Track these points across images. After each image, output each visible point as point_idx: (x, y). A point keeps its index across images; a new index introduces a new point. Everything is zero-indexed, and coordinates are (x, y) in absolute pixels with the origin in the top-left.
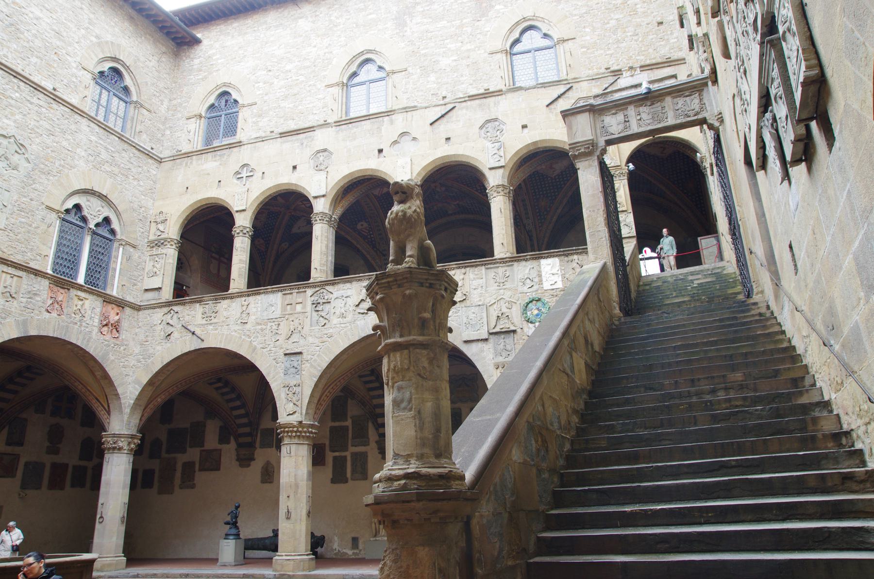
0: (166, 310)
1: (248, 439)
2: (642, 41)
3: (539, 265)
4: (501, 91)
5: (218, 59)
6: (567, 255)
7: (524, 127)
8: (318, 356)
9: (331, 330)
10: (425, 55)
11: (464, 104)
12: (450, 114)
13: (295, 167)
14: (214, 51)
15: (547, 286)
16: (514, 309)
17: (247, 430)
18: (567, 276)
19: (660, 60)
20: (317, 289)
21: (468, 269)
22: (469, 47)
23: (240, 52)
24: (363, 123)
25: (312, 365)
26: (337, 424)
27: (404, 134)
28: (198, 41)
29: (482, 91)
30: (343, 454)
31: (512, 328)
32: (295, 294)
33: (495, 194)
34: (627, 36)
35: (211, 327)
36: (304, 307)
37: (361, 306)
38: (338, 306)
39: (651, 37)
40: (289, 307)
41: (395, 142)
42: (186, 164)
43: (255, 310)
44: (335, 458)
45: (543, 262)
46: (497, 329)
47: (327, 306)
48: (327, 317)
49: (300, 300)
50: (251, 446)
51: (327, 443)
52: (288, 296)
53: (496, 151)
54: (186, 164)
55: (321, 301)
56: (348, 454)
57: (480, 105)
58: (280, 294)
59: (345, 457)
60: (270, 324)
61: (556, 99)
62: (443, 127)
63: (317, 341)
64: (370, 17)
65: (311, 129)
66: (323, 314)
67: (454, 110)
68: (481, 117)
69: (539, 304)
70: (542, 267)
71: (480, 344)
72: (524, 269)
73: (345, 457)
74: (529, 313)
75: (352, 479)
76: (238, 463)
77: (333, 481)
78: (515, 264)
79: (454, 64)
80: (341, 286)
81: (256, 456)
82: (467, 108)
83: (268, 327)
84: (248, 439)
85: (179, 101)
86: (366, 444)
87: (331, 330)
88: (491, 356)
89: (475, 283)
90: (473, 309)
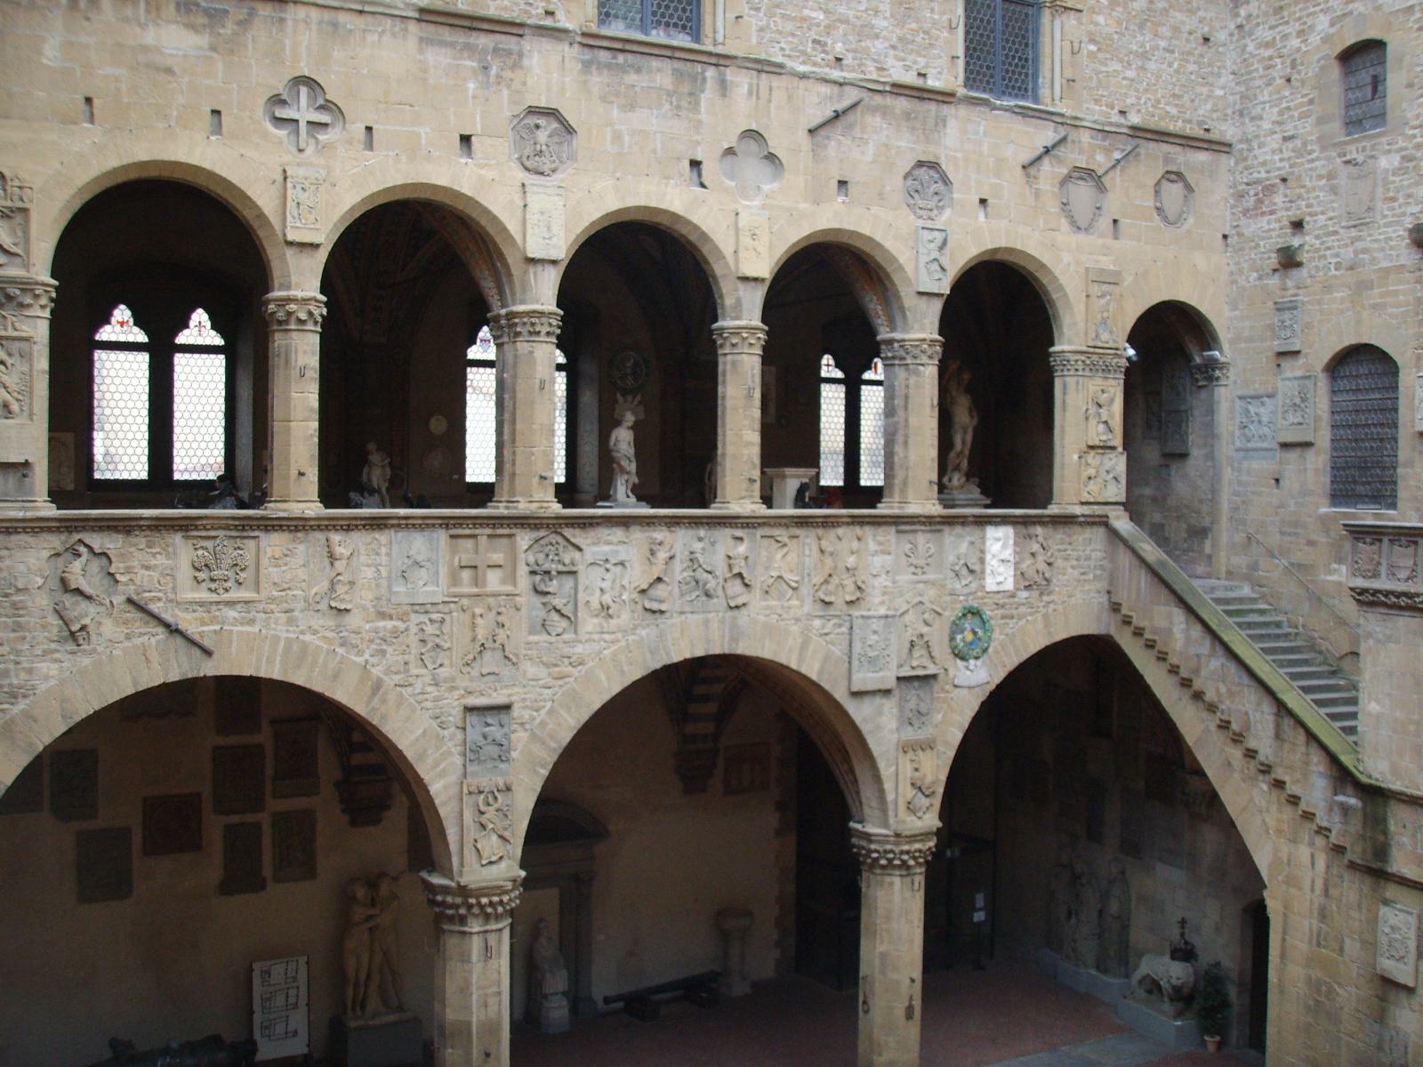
0: (56, 541)
2: (1177, 71)
3: (983, 538)
4: (952, 95)
7: (983, 202)
8: (551, 712)
9: (579, 649)
11: (878, 99)
12: (851, 117)
13: (466, 140)
15: (990, 584)
16: (937, 624)
18: (1024, 566)
20: (542, 533)
24: (655, 63)
25: (534, 737)
26: (232, 740)
27: (751, 134)
30: (250, 818)
31: (932, 670)
32: (483, 540)
33: (924, 359)
34: (1156, 48)
35: (232, 614)
36: (512, 578)
37: (652, 592)
38: (594, 584)
39: (1191, 67)
40: (466, 575)
41: (730, 152)
44: (230, 830)
47: (569, 583)
48: (567, 610)
49: (497, 557)
53: (935, 254)
55: (554, 567)
56: (264, 819)
59: (258, 826)
60: (415, 618)
61: (1039, 158)
63: (542, 672)
66: (558, 602)
67: (859, 109)
68: (908, 147)
69: (977, 620)
70: (988, 543)
71: (878, 700)
72: (957, 543)
74: (959, 637)
75: (277, 880)
77: (229, 886)
78: (947, 529)
83: (414, 629)
87: (579, 649)
88: (894, 725)
89: (878, 561)
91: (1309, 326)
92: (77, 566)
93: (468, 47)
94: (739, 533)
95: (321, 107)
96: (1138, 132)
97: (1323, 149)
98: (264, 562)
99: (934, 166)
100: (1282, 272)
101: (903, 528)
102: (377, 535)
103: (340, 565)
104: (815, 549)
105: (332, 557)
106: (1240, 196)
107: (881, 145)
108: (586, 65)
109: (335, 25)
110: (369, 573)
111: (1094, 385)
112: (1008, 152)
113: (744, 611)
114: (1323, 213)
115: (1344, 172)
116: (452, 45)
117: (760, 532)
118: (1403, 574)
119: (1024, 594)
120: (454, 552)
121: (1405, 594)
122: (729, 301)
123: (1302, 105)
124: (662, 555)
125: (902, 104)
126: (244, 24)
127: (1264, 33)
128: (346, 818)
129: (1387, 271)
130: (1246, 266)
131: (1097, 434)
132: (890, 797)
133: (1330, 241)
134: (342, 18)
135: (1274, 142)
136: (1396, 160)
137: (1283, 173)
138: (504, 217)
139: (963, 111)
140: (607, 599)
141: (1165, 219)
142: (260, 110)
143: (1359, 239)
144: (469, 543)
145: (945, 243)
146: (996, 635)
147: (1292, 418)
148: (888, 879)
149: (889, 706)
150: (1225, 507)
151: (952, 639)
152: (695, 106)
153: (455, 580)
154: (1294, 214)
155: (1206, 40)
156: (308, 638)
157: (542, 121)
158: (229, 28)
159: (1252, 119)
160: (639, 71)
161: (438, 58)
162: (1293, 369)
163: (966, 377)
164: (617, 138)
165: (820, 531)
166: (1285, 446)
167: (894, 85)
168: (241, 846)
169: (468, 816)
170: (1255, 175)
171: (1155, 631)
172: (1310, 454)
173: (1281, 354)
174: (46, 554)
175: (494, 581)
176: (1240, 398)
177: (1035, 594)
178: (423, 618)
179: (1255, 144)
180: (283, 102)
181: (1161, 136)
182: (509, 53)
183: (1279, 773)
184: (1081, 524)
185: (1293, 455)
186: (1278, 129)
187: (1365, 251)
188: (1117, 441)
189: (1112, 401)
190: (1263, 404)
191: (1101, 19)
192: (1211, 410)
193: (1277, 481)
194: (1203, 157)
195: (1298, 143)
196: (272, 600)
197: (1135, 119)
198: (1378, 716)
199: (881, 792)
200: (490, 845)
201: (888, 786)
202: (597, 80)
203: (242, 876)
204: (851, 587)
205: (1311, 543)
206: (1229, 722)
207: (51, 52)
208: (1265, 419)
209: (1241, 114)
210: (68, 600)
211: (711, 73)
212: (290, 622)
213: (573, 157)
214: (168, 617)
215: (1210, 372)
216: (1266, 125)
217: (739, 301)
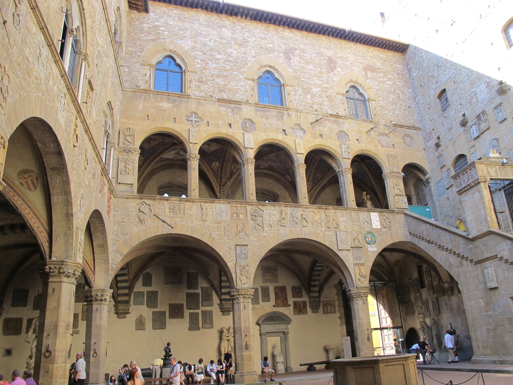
0: (139, 201)
1: (126, 298)
3: (370, 215)
5: (163, 31)
6: (381, 212)
10: (303, 81)
11: (327, 118)
13: (230, 125)
14: (160, 24)
15: (374, 226)
17: (126, 291)
19: (411, 126)
20: (253, 206)
21: (337, 211)
22: (325, 85)
23: (181, 33)
24: (272, 110)
28: (146, 11)
29: (335, 113)
30: (196, 311)
31: (361, 246)
32: (239, 208)
33: (347, 173)
40: (235, 215)
41: (292, 128)
42: (145, 98)
43: (211, 213)
45: (372, 214)
46: (353, 246)
48: (261, 225)
49: (243, 212)
50: (127, 302)
51: (185, 303)
52: (234, 208)
54: (145, 98)
57: (335, 121)
58: (229, 205)
59: (198, 313)
62: (318, 128)
64: (269, 45)
65: (239, 103)
68: (336, 128)
72: (363, 215)
73: (198, 313)
76: (116, 315)
77: (190, 329)
79: (320, 93)
80: (268, 207)
81: (130, 311)
82: (329, 120)
83: (222, 226)
84: (126, 298)
85: (134, 49)
86: (211, 305)
87: (264, 234)
88: (352, 260)
89: (341, 219)
90: (343, 233)
91: (446, 158)
92: (143, 207)
93: (229, 107)
94: (304, 209)
95: (197, 118)
96: (394, 125)
97: (439, 118)
98: (186, 209)
99: (344, 132)
101: (347, 211)
102: (213, 204)
103: (204, 210)
104: (324, 215)
105: (202, 208)
106: (425, 138)
107: (328, 127)
108: (256, 111)
109: (200, 102)
110: (211, 213)
111: (395, 181)
112: (362, 129)
113: (307, 228)
116: (226, 106)
117: (309, 210)
118: (466, 181)
119: (384, 230)
120: (232, 210)
121: (468, 185)
122: (295, 159)
124: (284, 213)
125: (333, 119)
126: (180, 102)
127: (422, 101)
128: (221, 313)
129: (458, 136)
131: (397, 192)
132: (354, 278)
134: (201, 101)
136: (454, 111)
138: (240, 140)
139: (349, 120)
140: (271, 223)
141: (407, 145)
142: (184, 118)
144: (236, 208)
145: (348, 147)
146: (378, 239)
147: (447, 181)
148: (357, 302)
149: (350, 254)
150: (438, 211)
151: (365, 239)
152: (283, 119)
153: (232, 216)
155: (410, 107)
156: (196, 226)
157: (247, 121)
158: (177, 103)
160: (268, 112)
161: (223, 109)
162: (444, 170)
163: (369, 196)
164: (265, 125)
165: (325, 210)
166: (447, 189)
167: (330, 115)
168: (194, 318)
169: (238, 271)
172: (453, 187)
173: (442, 168)
174: (136, 204)
175: (241, 216)
177: (387, 230)
178: (225, 224)
180: (189, 117)
181: (401, 126)
182: (239, 108)
184: (398, 213)
185: (450, 190)
188: (404, 194)
189: (400, 184)
191: (381, 103)
192: (430, 191)
194: (414, 131)
195: (434, 120)
196: (187, 217)
197: (393, 123)
199: (351, 277)
200: (244, 279)
201: (353, 275)
202: (259, 113)
203: (194, 326)
204: (335, 224)
205: (459, 209)
207: (140, 107)
210: (141, 214)
211: (286, 112)
212: (192, 222)
213: (255, 128)
214: (163, 219)
215: (427, 182)
217: (298, 159)
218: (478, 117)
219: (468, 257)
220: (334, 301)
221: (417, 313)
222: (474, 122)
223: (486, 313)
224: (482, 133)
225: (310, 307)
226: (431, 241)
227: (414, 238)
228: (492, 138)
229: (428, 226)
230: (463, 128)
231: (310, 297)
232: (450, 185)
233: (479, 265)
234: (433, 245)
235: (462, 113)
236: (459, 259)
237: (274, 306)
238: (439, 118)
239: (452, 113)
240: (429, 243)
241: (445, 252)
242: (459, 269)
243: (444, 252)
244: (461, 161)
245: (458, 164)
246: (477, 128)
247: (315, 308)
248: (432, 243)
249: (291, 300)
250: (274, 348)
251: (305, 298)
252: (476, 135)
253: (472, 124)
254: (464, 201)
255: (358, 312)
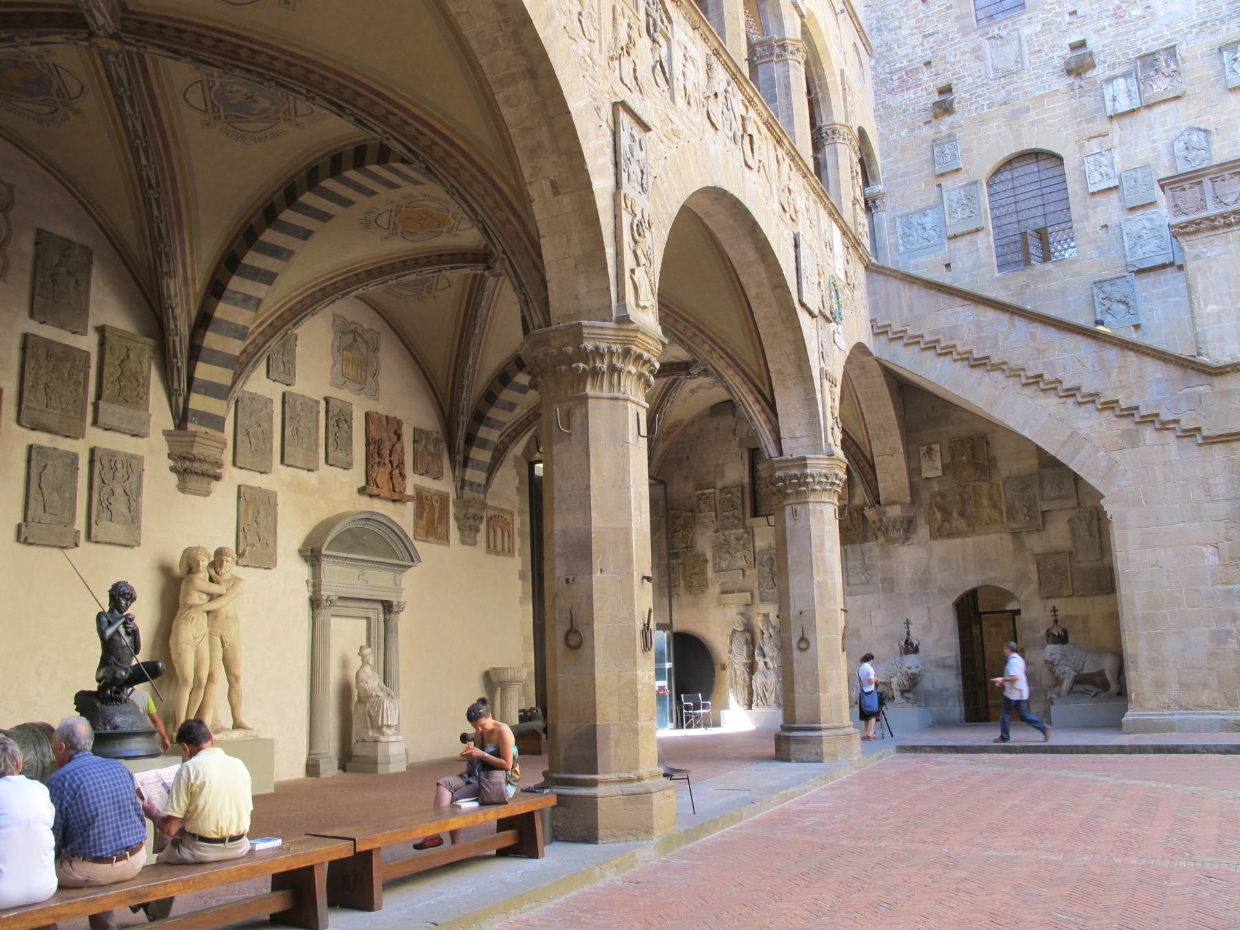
56: (80, 448)
59: (74, 458)
73: (74, 458)
97: (965, 34)
100: (935, 122)
114: (970, 75)
115: (987, 44)
118: (1230, 200)
121: (1234, 212)
123: (939, 12)
128: (174, 478)
130: (896, 126)
133: (979, 91)
135: (917, 39)
137: (927, 59)
143: (1011, 83)
154: (941, 82)
159: (891, 30)
170: (898, 65)
171: (936, 332)
172: (980, 235)
176: (900, 217)
179: (895, 46)
183: (1109, 396)
185: (962, 243)
186: (915, 31)
187: (1016, 89)
190: (925, 215)
193: (948, 266)
198: (1218, 315)
206: (1041, 376)
208: (928, 225)
209: (879, 30)
216: (905, 32)
218: (1148, 61)
219: (1177, 421)
220: (512, 513)
221: (714, 590)
222: (1119, 70)
223: (1220, 587)
224: (1149, 107)
225: (457, 519)
226: (995, 360)
227: (897, 347)
228: (1184, 125)
229: (990, 314)
230: (1070, 80)
231: (463, 484)
232: (972, 227)
233: (1215, 447)
234: (997, 375)
235: (1075, 39)
236: (1126, 424)
237: (362, 491)
238: (965, 34)
239: (1026, 31)
240: (972, 367)
241: (1055, 400)
242: (1117, 456)
243: (1051, 403)
244: (1026, 169)
245: (1001, 177)
246: (1134, 89)
247: (468, 529)
248: (996, 367)
249: (413, 481)
250: (345, 664)
251: (445, 486)
252: (1123, 105)
253: (1109, 73)
254: (1197, 257)
255: (822, 546)
